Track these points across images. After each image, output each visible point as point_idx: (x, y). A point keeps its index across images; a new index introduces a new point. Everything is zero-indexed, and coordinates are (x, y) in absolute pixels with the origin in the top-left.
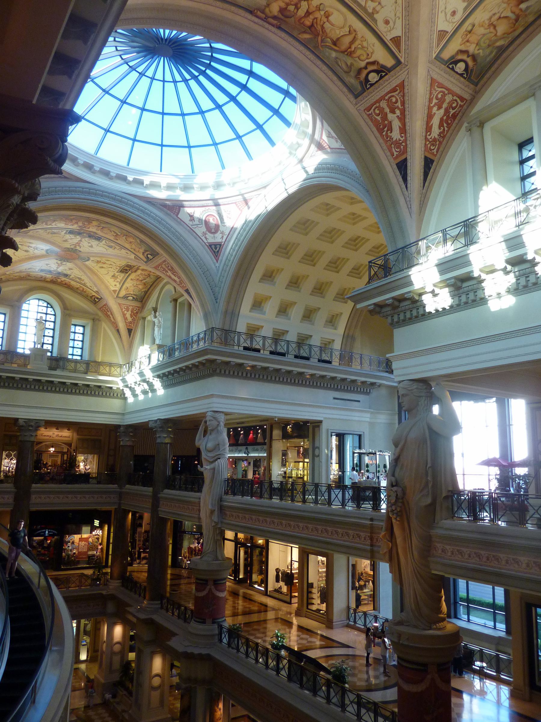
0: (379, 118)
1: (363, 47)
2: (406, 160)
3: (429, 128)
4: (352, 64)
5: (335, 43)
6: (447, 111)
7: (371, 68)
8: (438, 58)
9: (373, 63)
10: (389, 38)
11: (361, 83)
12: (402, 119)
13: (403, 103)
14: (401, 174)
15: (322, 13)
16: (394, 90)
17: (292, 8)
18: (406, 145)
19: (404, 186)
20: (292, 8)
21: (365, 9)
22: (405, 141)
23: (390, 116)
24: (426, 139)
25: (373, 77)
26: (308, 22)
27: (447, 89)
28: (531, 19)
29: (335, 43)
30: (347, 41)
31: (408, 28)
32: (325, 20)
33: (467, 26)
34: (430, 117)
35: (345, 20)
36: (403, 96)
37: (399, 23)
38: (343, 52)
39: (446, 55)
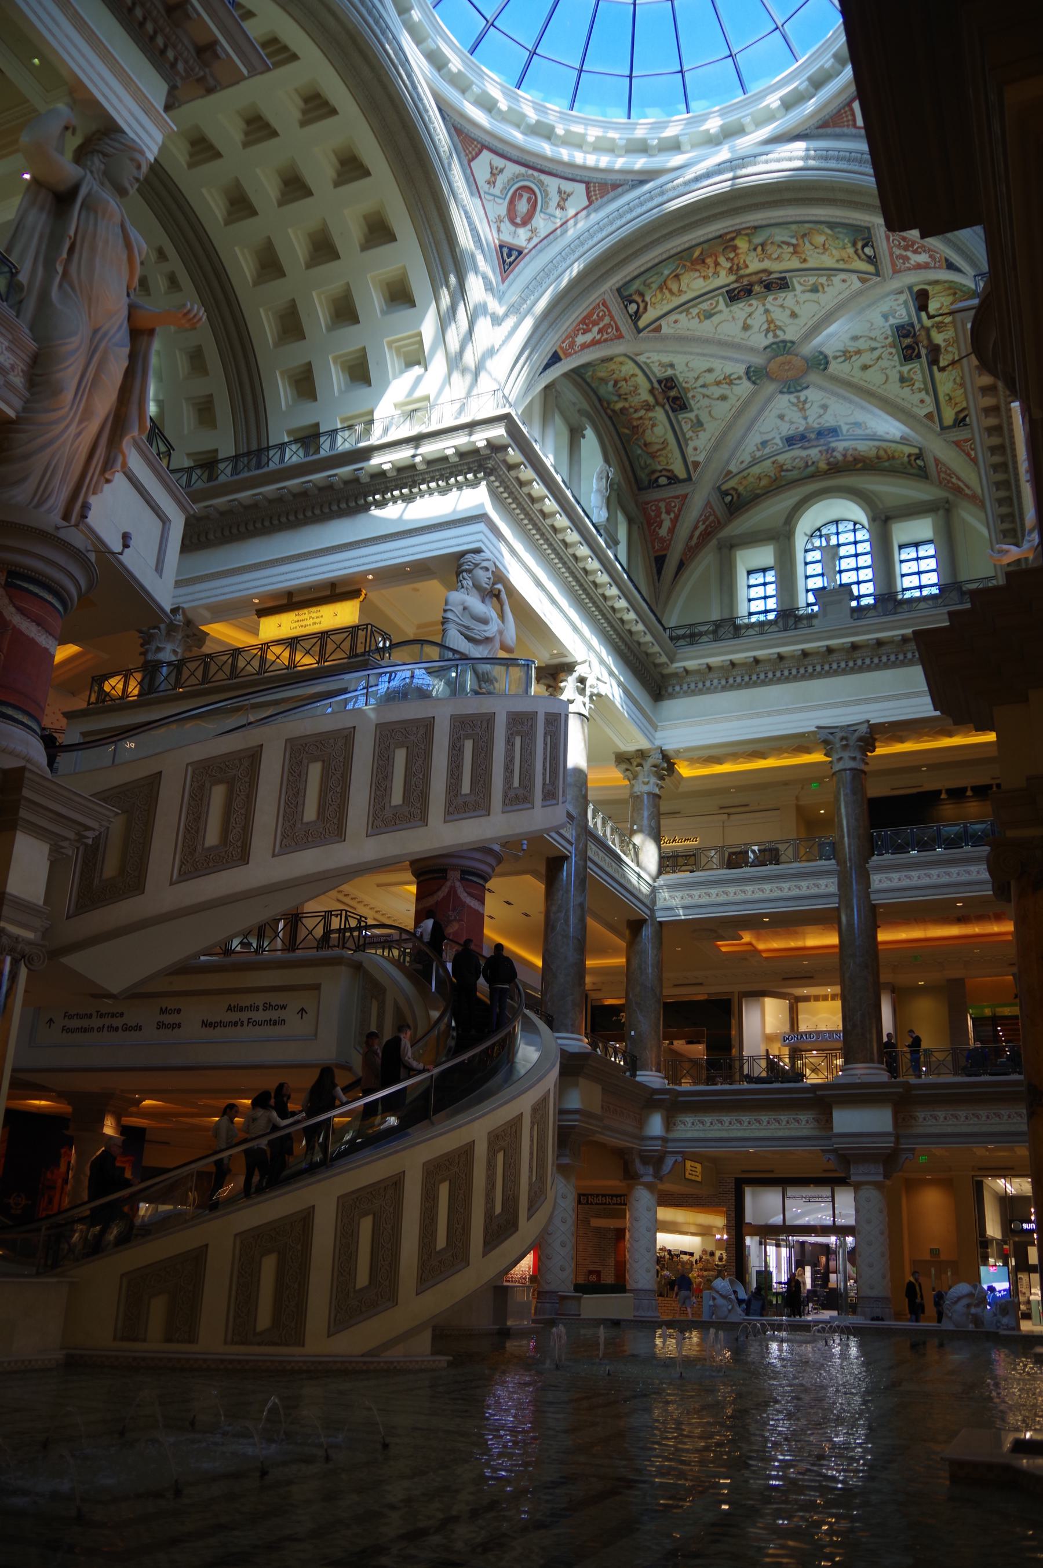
0: (653, 514)
1: (667, 457)
2: (665, 556)
3: (691, 537)
4: (650, 465)
5: (646, 445)
6: (707, 527)
7: (664, 473)
8: (719, 488)
9: (669, 471)
11: (650, 481)
12: (674, 522)
13: (680, 510)
14: (656, 565)
15: (651, 422)
16: (677, 497)
17: (632, 410)
18: (669, 544)
19: (656, 578)
20: (632, 410)
21: (684, 435)
22: (671, 539)
23: (664, 516)
24: (687, 545)
25: (663, 481)
26: (635, 424)
27: (714, 512)
28: (784, 483)
32: (650, 427)
33: (745, 473)
34: (696, 528)
35: (665, 433)
36: (683, 505)
38: (648, 453)
39: (724, 488)
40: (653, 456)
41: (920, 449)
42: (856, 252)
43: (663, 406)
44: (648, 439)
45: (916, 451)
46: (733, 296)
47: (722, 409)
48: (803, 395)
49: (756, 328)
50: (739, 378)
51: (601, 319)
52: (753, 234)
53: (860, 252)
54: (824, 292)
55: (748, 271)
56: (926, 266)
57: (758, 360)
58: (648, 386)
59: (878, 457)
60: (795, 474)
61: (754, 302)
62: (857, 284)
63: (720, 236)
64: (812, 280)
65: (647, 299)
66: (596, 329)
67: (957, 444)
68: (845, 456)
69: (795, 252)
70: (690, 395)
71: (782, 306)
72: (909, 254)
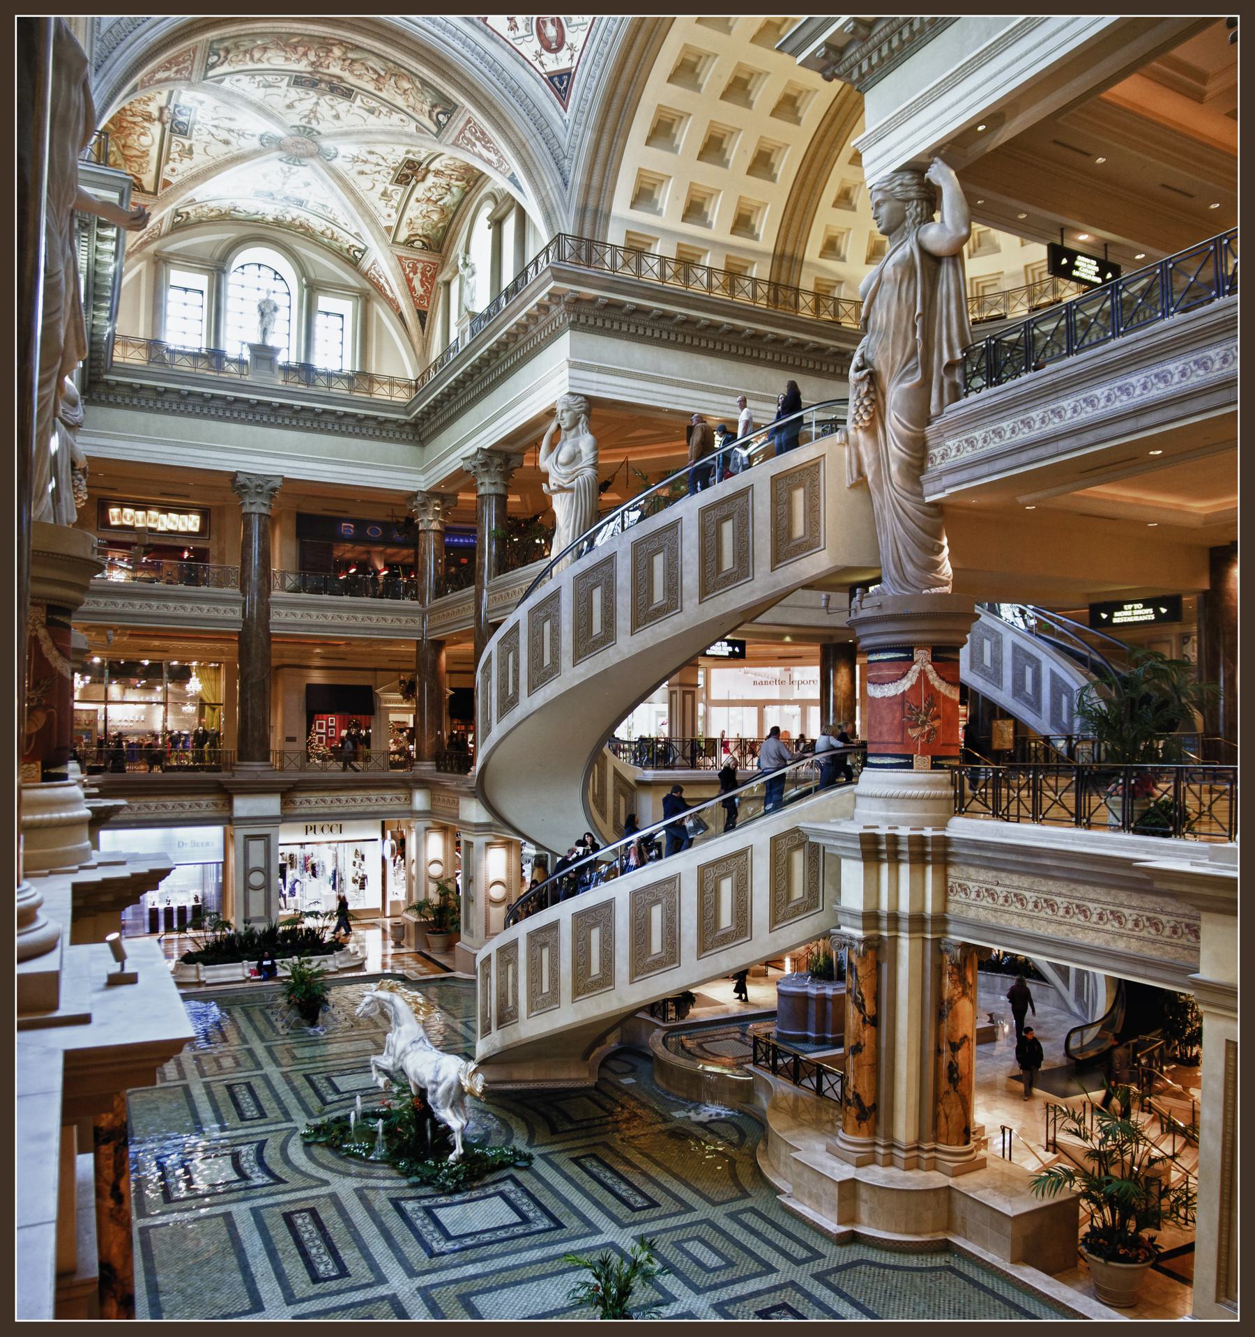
10: (165, 177)
21: (169, 152)
29: (124, 146)
30: (135, 153)
31: (182, 185)
37: (180, 177)
40: (127, 159)
41: (367, 248)
42: (430, 112)
43: (163, 124)
44: (130, 141)
45: (363, 247)
46: (299, 81)
47: (218, 151)
48: (295, 169)
49: (297, 111)
50: (253, 135)
51: (184, 61)
52: (352, 50)
53: (434, 114)
54: (378, 117)
55: (326, 71)
56: (489, 162)
57: (278, 132)
58: (163, 104)
59: (323, 233)
60: (242, 215)
61: (312, 93)
62: (412, 127)
63: (324, 38)
64: (374, 104)
65: (230, 56)
66: (175, 69)
67: (400, 258)
68: (294, 220)
69: (377, 80)
70: (196, 127)
71: (332, 107)
72: (478, 143)
